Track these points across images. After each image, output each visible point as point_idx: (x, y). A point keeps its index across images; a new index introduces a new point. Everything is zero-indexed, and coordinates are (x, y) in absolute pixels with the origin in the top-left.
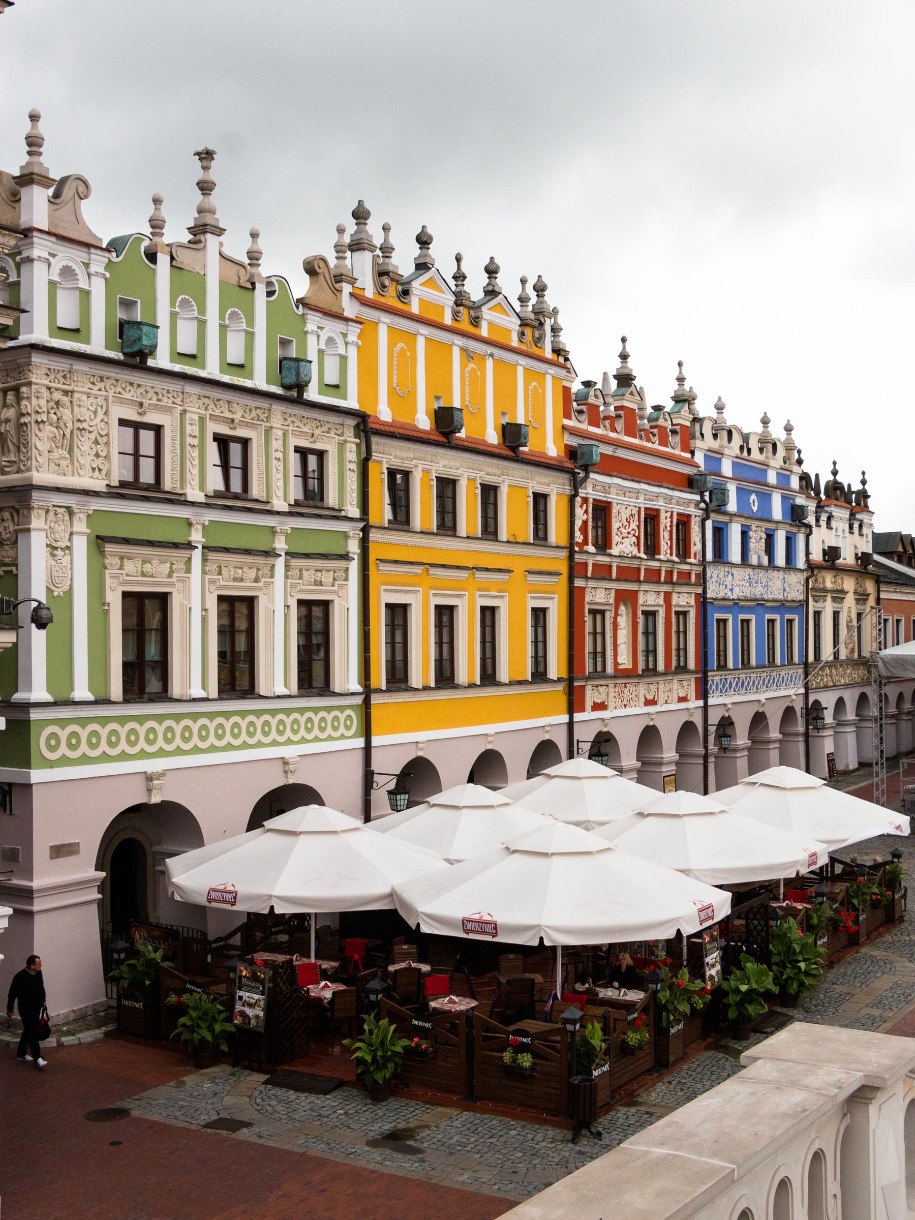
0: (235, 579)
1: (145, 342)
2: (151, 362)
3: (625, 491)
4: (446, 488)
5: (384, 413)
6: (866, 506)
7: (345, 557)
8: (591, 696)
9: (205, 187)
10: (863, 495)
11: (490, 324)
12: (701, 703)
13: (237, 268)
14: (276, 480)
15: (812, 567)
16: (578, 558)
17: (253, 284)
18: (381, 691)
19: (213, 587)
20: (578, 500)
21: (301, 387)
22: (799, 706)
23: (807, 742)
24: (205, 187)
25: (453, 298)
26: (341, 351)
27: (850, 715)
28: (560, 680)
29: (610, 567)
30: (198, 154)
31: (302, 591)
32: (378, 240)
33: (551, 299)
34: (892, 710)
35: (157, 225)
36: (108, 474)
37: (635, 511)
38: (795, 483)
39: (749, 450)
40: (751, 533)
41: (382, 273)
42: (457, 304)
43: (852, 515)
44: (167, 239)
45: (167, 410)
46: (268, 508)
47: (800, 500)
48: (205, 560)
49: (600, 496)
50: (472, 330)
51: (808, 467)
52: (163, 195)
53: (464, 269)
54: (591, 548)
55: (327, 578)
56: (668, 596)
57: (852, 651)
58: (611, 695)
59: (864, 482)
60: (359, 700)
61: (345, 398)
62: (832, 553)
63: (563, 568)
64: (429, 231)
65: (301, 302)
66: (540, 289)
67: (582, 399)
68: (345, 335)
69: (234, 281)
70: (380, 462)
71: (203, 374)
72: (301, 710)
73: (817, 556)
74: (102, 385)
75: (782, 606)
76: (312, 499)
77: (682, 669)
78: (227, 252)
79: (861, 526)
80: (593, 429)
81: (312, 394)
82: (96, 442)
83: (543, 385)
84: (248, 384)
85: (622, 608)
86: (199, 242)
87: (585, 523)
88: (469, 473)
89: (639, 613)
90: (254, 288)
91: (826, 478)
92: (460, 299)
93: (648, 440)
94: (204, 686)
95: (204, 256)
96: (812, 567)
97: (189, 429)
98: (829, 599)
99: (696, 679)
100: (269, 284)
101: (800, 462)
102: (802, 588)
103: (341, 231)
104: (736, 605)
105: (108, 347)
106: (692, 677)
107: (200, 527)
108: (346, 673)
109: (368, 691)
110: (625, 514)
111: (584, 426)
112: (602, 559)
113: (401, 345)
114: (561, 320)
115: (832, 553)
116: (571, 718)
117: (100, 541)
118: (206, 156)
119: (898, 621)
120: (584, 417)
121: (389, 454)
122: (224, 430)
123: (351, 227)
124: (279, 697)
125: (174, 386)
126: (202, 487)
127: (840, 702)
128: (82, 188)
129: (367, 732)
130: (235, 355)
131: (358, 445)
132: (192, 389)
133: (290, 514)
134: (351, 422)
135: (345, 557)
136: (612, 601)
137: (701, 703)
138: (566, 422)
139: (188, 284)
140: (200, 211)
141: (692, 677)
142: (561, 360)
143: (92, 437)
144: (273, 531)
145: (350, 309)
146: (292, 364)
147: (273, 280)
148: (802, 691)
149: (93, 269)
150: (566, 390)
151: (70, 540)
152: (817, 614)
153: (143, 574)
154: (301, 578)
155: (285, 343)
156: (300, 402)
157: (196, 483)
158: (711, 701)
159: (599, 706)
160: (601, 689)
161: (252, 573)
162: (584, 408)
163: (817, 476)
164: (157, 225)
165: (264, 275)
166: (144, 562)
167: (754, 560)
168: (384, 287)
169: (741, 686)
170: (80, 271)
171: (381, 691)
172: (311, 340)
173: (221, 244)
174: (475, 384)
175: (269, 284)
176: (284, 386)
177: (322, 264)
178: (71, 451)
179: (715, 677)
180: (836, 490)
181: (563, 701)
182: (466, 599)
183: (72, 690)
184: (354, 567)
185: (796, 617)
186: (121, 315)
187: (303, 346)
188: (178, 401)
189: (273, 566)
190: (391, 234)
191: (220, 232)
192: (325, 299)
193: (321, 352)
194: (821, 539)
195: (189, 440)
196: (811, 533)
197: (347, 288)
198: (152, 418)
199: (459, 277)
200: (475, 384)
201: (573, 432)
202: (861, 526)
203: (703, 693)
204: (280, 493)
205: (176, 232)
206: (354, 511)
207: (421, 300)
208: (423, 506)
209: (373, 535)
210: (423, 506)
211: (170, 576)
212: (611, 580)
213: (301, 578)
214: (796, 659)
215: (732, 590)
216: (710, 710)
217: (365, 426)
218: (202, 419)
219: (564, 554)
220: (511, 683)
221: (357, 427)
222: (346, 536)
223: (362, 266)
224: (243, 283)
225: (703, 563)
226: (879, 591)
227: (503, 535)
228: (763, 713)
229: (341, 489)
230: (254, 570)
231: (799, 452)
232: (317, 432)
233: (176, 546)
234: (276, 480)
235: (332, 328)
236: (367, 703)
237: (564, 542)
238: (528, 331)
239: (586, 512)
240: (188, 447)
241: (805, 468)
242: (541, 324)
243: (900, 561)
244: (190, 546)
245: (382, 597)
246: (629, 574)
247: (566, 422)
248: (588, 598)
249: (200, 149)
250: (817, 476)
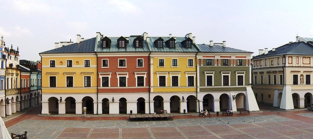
6: (18, 54)
10: (18, 52)
15: (7, 68)
22: (4, 99)
23: (5, 107)
27: (15, 101)
34: (23, 99)
38: (3, 50)
43: (15, 57)
47: (5, 54)
51: (7, 46)
57: (15, 86)
59: (18, 49)
62: (11, 65)
73: (8, 66)
79: (17, 59)
91: (10, 48)
96: (7, 68)
98: (10, 75)
101: (5, 45)
102: (5, 73)
115: (11, 65)
119: (25, 80)
127: (13, 98)
148: (5, 96)
152: (8, 79)
163: (8, 48)
180: (12, 50)
185: (3, 79)
194: (9, 62)
196: (7, 61)
202: (17, 59)
214: (3, 89)
226: (21, 73)
231: (4, 43)
241: (6, 46)
243: (25, 66)
250: (8, 48)
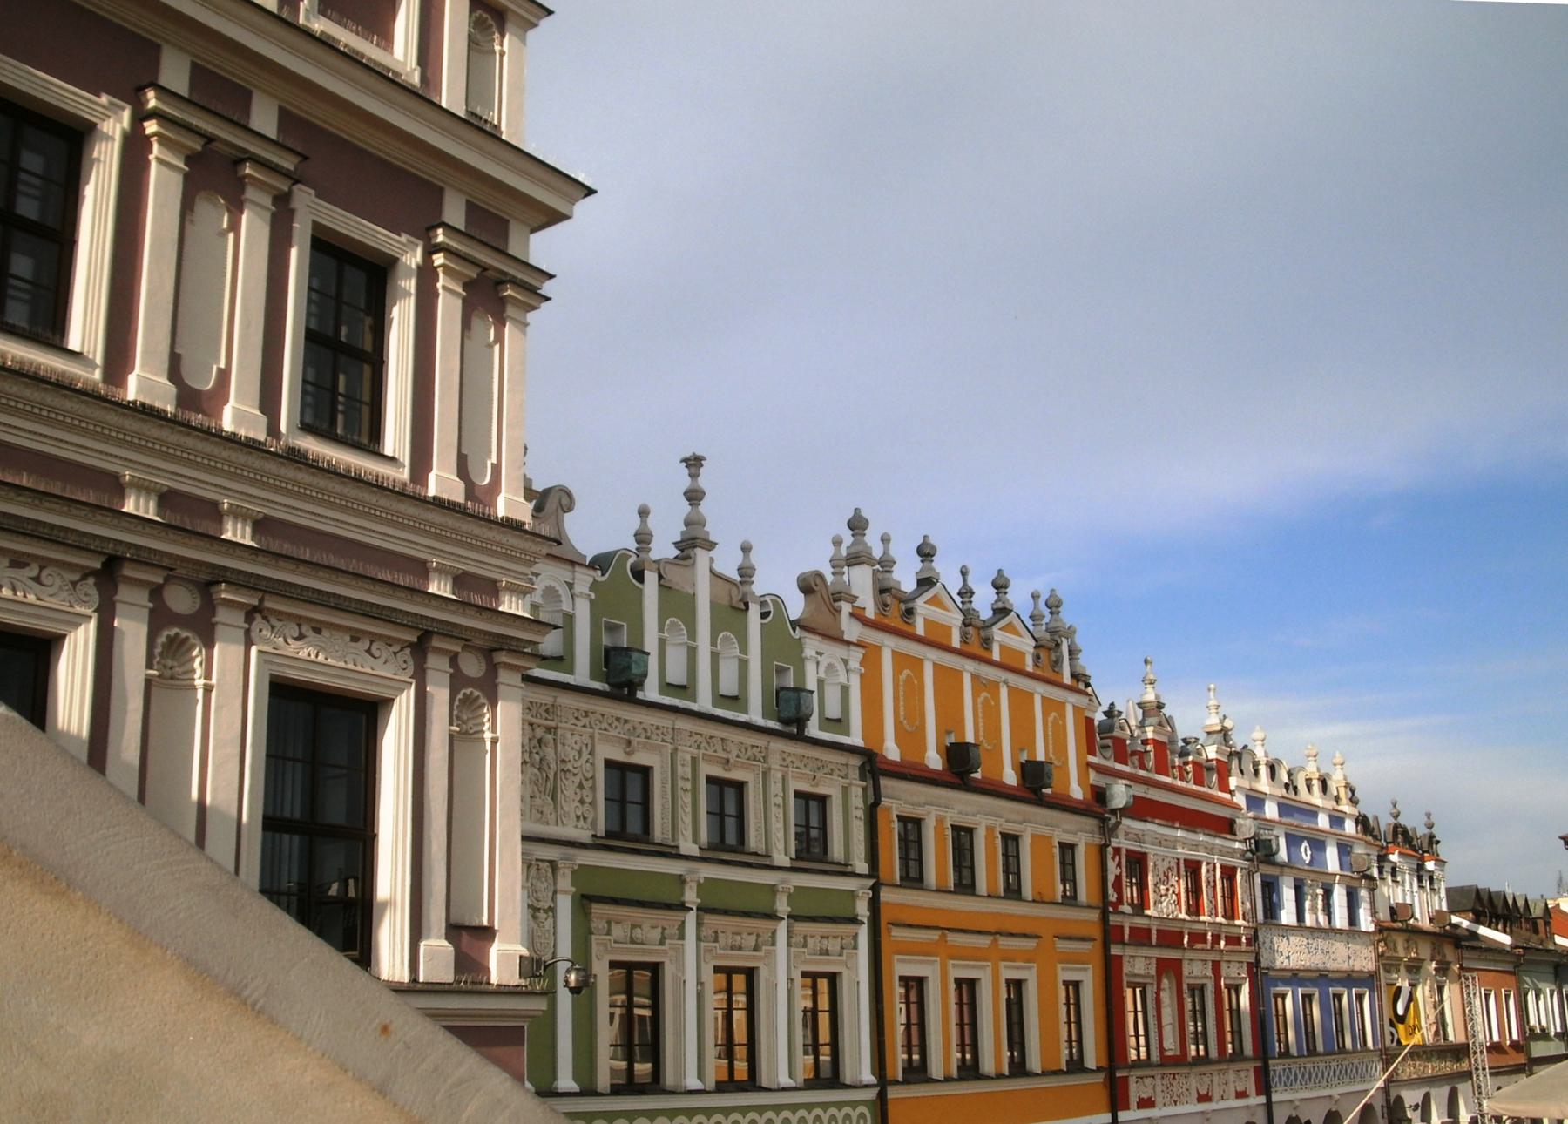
0: (732, 948)
1: (635, 670)
2: (640, 695)
3: (1160, 842)
4: (963, 838)
5: (892, 751)
7: (854, 920)
8: (1135, 1091)
9: (694, 496)
11: (1003, 648)
12: (1262, 1099)
13: (728, 586)
14: (771, 828)
16: (1114, 920)
17: (747, 604)
18: (896, 1082)
19: (709, 956)
20: (1110, 850)
21: (801, 721)
24: (694, 496)
25: (961, 617)
26: (843, 679)
28: (1099, 1069)
29: (1149, 930)
30: (685, 460)
31: (806, 962)
32: (877, 552)
33: (1067, 617)
35: (643, 538)
36: (594, 824)
37: (1173, 864)
39: (1295, 788)
40: (1306, 889)
41: (884, 590)
42: (966, 624)
44: (655, 554)
45: (656, 749)
46: (767, 862)
48: (699, 924)
49: (1135, 846)
50: (982, 653)
52: (652, 506)
53: (971, 583)
54: (1126, 908)
55: (834, 945)
56: (1216, 967)
58: (1159, 1089)
60: (871, 1094)
61: (847, 734)
63: (1096, 932)
64: (932, 540)
65: (795, 624)
66: (1054, 606)
67: (1106, 728)
68: (845, 662)
69: (725, 602)
70: (889, 809)
71: (694, 707)
72: (809, 1107)
74: (585, 721)
75: (1350, 979)
76: (812, 849)
77: (1238, 1055)
78: (718, 568)
80: (1119, 767)
81: (813, 730)
82: (581, 786)
83: (1063, 716)
84: (742, 717)
85: (1165, 982)
86: (688, 557)
87: (1118, 878)
88: (987, 818)
89: (1185, 987)
90: (747, 608)
91: (1385, 822)
92: (969, 618)
93: (1182, 779)
94: (700, 1076)
95: (694, 575)
97: (680, 770)
99: (1256, 1069)
100: (763, 604)
103: (837, 542)
104: (1295, 977)
105: (593, 677)
106: (1251, 1066)
107: (694, 885)
109: (883, 1082)
110: (1162, 867)
111: (1111, 764)
112: (1139, 921)
113: (906, 672)
114: (1079, 640)
116: (1115, 1117)
117: (584, 902)
118: (694, 463)
120: (1109, 753)
121: (900, 798)
122: (718, 772)
123: (848, 538)
124: (784, 1089)
125: (664, 721)
126: (695, 840)
128: (565, 501)
130: (729, 686)
131: (865, 789)
132: (684, 724)
133: (793, 869)
134: (856, 761)
135: (854, 920)
136: (1153, 972)
137: (1262, 1099)
138: (1091, 759)
139: (677, 604)
140: (687, 524)
141: (1251, 1066)
142: (1081, 686)
143: (577, 780)
144: (772, 890)
145: (852, 630)
146: (791, 694)
147: (767, 599)
149: (578, 589)
150: (1089, 721)
151: (554, 899)
153: (633, 941)
154: (805, 946)
155: (781, 671)
156: (801, 738)
157: (689, 834)
158: (1275, 1097)
159: (1146, 1103)
160: (1148, 1081)
161: (751, 941)
162: (1109, 742)
163: (1376, 818)
164: (643, 538)
165: (758, 594)
166: (633, 927)
168: (886, 605)
169: (1309, 1079)
170: (563, 592)
171: (896, 1082)
172: (810, 669)
173: (712, 560)
174: (989, 715)
175: (763, 604)
176: (780, 720)
177: (818, 581)
178: (554, 798)
179: (1276, 1066)
180: (1401, 835)
181: (1102, 1096)
182: (989, 970)
183: (555, 1079)
184: (863, 933)
186: (606, 641)
187: (801, 674)
188: (668, 738)
189: (774, 933)
190: (892, 545)
191: (711, 546)
192: (823, 619)
193: (821, 682)
195: (680, 783)
197: (846, 608)
198: (640, 758)
199: (967, 593)
200: (989, 715)
201: (1100, 769)
203: (1264, 1087)
204: (781, 846)
205: (663, 548)
206: (862, 867)
207: (926, 620)
208: (936, 860)
209: (886, 895)
210: (936, 860)
211: (662, 943)
212: (1151, 945)
213: (805, 946)
216: (1275, 1109)
217: (872, 765)
218: (694, 760)
219: (1094, 915)
220: (1044, 1074)
221: (862, 768)
222: (852, 895)
223: (861, 581)
224: (735, 603)
227: (1028, 891)
228: (1337, 1112)
229: (846, 836)
230: (754, 937)
232: (819, 775)
233: (668, 907)
234: (771, 828)
235: (833, 652)
236: (882, 1096)
237: (1096, 901)
238: (1043, 654)
239: (1119, 865)
240: (680, 792)
242: (1058, 645)
244: (683, 907)
245: (900, 967)
246: (1170, 937)
247: (1091, 759)
248: (1126, 969)
249: (688, 454)
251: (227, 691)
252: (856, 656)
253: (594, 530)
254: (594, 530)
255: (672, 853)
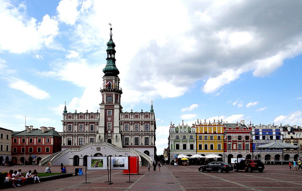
9: (183, 122)
24: (183, 122)
54: (227, 139)
63: (223, 141)
108: (195, 148)
109: (197, 150)
117: (174, 142)
118: (183, 121)
129: (197, 152)
145: (196, 126)
167: (266, 139)
206: (195, 139)
210: (203, 138)
215: (260, 142)
217: (196, 133)
225: (252, 140)
235: (194, 128)
236: (197, 150)
251: (144, 137)
252: (196, 128)
253: (176, 126)
254: (176, 126)
255: (180, 139)
